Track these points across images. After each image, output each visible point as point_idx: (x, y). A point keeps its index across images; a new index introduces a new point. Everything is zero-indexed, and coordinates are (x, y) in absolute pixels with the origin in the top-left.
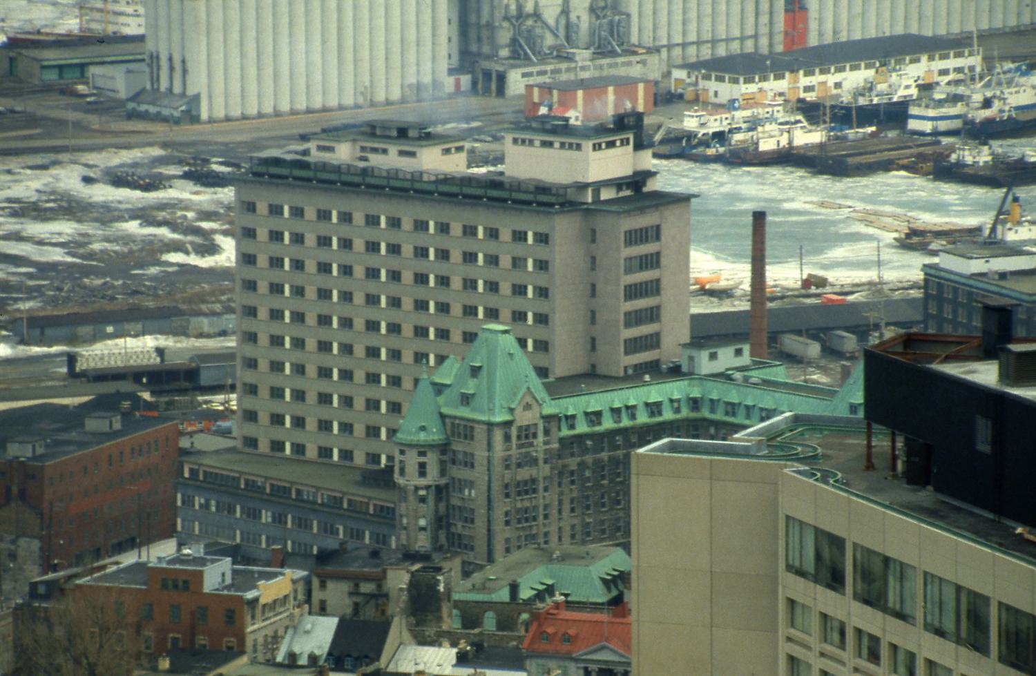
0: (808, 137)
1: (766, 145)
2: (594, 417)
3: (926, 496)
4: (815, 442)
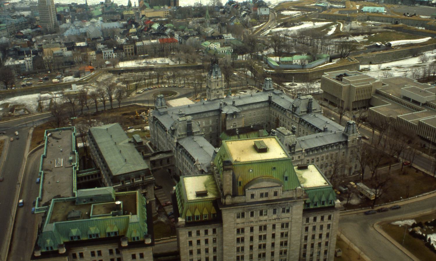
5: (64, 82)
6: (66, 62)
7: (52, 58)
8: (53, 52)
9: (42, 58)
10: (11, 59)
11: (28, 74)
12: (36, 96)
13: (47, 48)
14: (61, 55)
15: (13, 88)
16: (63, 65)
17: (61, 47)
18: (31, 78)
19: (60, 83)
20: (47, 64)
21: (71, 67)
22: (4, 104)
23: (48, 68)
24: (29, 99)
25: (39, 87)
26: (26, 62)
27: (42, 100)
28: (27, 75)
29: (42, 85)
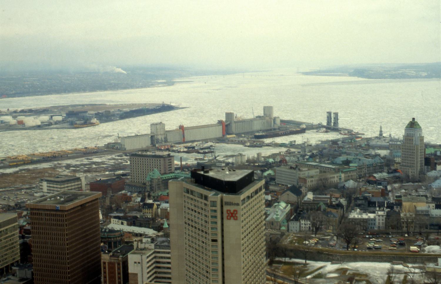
0: (185, 150)
1: (182, 151)
2: (165, 177)
3: (197, 184)
4: (186, 180)
5: (426, 253)
6: (432, 225)
7: (414, 216)
9: (399, 213)
10: (358, 210)
11: (377, 234)
12: (387, 265)
13: (408, 201)
14: (427, 214)
15: (356, 250)
16: (427, 228)
17: (427, 203)
18: (380, 240)
19: (420, 253)
20: (405, 223)
21: (438, 232)
22: (342, 269)
23: (405, 229)
24: (375, 269)
26: (377, 217)
27: (395, 273)
28: (376, 234)
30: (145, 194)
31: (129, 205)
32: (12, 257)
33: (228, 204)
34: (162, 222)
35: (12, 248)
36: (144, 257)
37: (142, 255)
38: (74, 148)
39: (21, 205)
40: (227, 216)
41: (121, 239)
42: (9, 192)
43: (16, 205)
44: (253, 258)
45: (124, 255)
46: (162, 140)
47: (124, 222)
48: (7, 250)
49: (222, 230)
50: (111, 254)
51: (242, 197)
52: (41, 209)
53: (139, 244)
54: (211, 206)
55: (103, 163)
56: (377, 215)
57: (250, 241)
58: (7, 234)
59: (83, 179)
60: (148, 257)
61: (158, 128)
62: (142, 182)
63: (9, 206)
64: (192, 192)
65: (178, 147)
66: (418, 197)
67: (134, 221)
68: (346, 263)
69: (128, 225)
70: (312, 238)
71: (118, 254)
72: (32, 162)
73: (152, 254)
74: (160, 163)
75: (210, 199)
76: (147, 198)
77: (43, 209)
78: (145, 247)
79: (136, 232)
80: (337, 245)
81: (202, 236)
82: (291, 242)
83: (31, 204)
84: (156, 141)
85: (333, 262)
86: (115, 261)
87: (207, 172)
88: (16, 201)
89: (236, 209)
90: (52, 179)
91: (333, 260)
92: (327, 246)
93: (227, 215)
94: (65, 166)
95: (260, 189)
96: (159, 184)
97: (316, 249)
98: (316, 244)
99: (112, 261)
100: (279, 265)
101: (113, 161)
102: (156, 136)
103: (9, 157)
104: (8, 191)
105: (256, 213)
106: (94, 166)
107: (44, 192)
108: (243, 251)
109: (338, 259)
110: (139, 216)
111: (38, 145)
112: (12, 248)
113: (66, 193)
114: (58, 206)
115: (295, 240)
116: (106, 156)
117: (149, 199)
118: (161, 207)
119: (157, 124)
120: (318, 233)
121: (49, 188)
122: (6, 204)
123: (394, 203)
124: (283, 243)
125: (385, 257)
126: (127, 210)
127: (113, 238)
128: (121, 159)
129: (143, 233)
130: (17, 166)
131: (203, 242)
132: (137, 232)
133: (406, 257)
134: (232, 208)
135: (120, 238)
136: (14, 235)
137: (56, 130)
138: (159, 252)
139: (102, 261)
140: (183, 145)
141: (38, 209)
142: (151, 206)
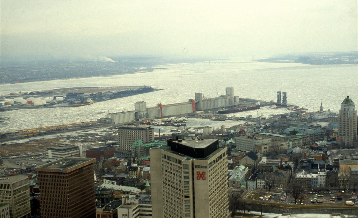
0: (163, 123)
1: (160, 124)
2: (147, 146)
3: (172, 151)
4: (164, 147)
7: (349, 176)
8: (350, 169)
9: (337, 173)
10: (304, 171)
11: (320, 191)
13: (344, 164)
15: (302, 204)
18: (322, 195)
20: (342, 181)
23: (342, 187)
25: (331, 207)
26: (319, 177)
28: (318, 191)
29: (335, 206)
30: (130, 159)
31: (117, 168)
32: (24, 211)
33: (197, 167)
34: (144, 181)
35: (24, 203)
36: (131, 210)
37: (128, 209)
38: (73, 122)
39: (31, 168)
40: (197, 177)
41: (112, 196)
42: (22, 159)
43: (27, 169)
44: (218, 211)
45: (114, 209)
46: (144, 116)
47: (114, 182)
48: (20, 205)
49: (193, 188)
50: (104, 208)
51: (209, 161)
52: (47, 172)
53: (126, 200)
54: (184, 169)
55: (96, 134)
56: (319, 175)
57: (216, 197)
58: (20, 192)
59: (81, 148)
60: (133, 210)
61: (140, 106)
62: (128, 150)
63: (22, 170)
64: (169, 158)
65: (157, 121)
66: (353, 161)
67: (122, 182)
68: (294, 214)
69: (117, 184)
70: (266, 194)
71: (110, 208)
72: (40, 134)
73: (137, 208)
74: (142, 134)
75: (183, 163)
76: (132, 163)
77: (49, 172)
78: (131, 203)
79: (123, 190)
80: (286, 200)
81: (177, 193)
82: (249, 197)
83: (39, 168)
84: (139, 116)
85: (284, 213)
86: (107, 214)
87: (181, 141)
88: (27, 166)
89: (204, 171)
90: (56, 148)
91: (284, 212)
92: (278, 201)
93: (197, 176)
94: (66, 137)
95: (224, 155)
96: (142, 152)
97: (270, 203)
98: (270, 199)
99: (105, 213)
100: (240, 216)
101: (105, 133)
102: (139, 113)
103: (21, 130)
104: (21, 157)
105: (220, 174)
106: (89, 137)
107: (49, 158)
108: (210, 205)
109: (288, 211)
110: (126, 178)
111: (44, 120)
112: (24, 203)
113: (67, 159)
114: (61, 169)
115: (253, 196)
116: (99, 128)
117: (134, 164)
118: (143, 170)
119: (140, 103)
120: (271, 190)
121: (53, 155)
122: (19, 168)
123: (333, 165)
124: (243, 199)
125: (326, 209)
126: (117, 172)
127: (106, 195)
128: (111, 131)
129: (129, 191)
130: (27, 137)
131: (178, 198)
132: (125, 190)
133: (343, 209)
134: (201, 170)
135: (110, 195)
136: (26, 193)
137: (59, 108)
138: (142, 207)
139: (97, 214)
140: (160, 119)
141: (45, 172)
142: (135, 169)
